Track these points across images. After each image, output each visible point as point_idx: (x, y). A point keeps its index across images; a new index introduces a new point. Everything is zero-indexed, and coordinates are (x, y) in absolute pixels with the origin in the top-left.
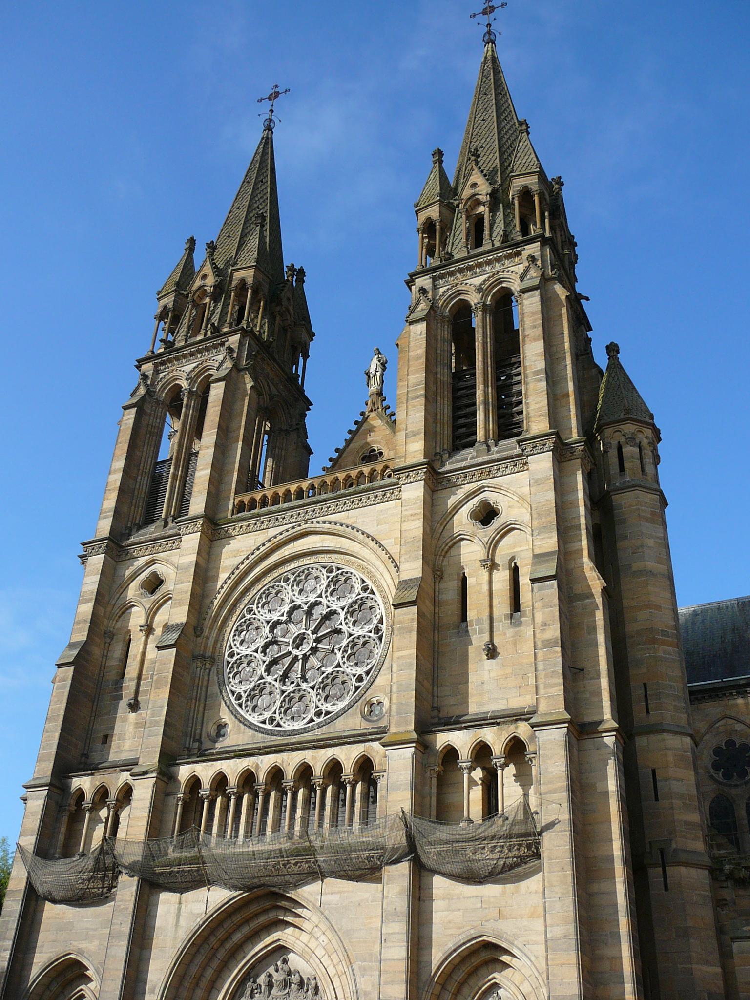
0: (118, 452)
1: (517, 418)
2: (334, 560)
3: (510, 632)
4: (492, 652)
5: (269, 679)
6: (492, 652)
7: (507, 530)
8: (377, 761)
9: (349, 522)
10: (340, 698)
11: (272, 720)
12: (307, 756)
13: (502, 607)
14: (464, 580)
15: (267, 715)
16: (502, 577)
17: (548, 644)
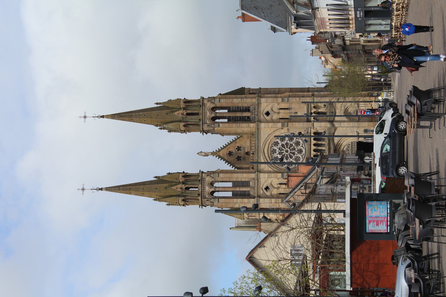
0: (232, 201)
1: (244, 108)
2: (270, 145)
3: (292, 110)
4: (296, 113)
5: (294, 157)
6: (296, 113)
7: (272, 110)
8: (315, 131)
9: (263, 141)
10: (300, 142)
11: (302, 156)
12: (312, 144)
13: (287, 111)
14: (280, 119)
15: (301, 157)
16: (281, 111)
17: (300, 99)
